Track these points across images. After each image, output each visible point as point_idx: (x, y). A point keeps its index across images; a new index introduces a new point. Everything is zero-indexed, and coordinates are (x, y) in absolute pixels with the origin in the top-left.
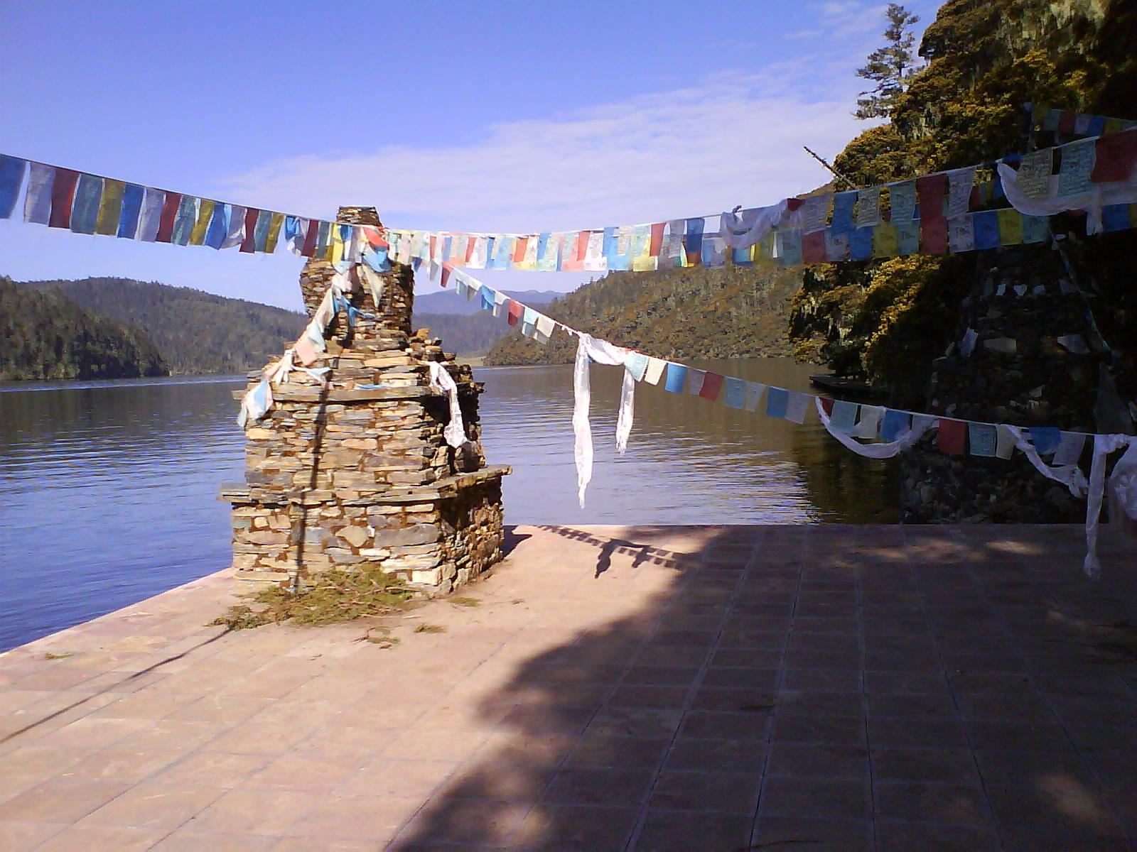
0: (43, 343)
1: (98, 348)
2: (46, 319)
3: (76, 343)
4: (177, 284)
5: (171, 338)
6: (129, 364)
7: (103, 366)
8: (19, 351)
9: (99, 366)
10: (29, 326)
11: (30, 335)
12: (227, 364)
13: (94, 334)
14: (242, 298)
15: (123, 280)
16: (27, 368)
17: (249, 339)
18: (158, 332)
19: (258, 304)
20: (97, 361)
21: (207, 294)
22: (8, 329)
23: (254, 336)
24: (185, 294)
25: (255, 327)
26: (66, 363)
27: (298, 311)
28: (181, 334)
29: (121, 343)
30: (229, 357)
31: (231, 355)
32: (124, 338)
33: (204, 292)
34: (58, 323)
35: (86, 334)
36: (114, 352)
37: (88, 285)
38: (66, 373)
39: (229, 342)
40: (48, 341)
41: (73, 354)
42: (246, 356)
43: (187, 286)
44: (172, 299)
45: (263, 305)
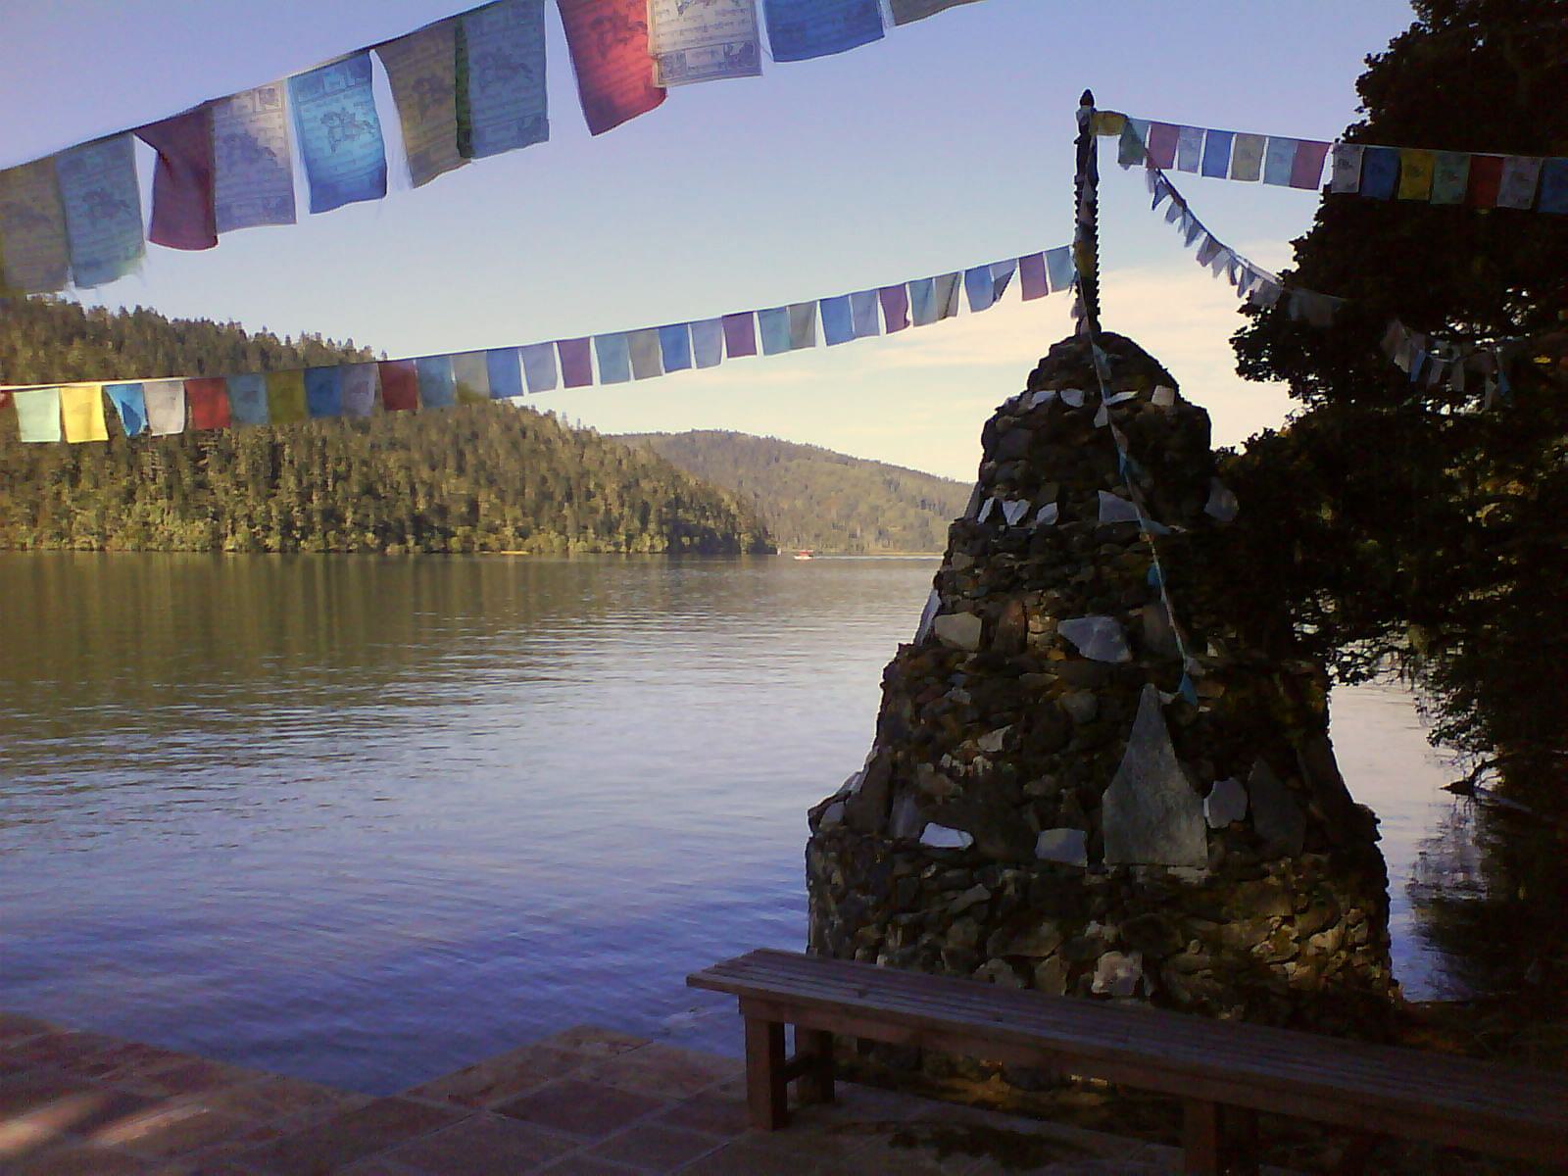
0: (626, 509)
1: (690, 516)
2: (631, 480)
3: (664, 510)
4: (798, 440)
5: (786, 507)
6: (727, 538)
7: (697, 540)
8: (600, 517)
9: (691, 540)
10: (612, 488)
11: (613, 500)
12: (854, 542)
13: (686, 499)
14: (878, 459)
15: (732, 433)
16: (607, 538)
17: (884, 511)
18: (770, 498)
19: (898, 467)
20: (689, 534)
21: (834, 452)
22: (588, 490)
23: (891, 508)
24: (808, 452)
25: (894, 496)
26: (652, 533)
27: (949, 477)
28: (799, 503)
29: (719, 511)
30: (858, 532)
31: (861, 530)
32: (723, 505)
33: (829, 450)
34: (645, 485)
35: (678, 499)
36: (711, 523)
37: (690, 441)
38: (652, 546)
39: (859, 515)
40: (632, 506)
41: (661, 522)
42: (880, 533)
43: (809, 443)
44: (790, 459)
45: (904, 468)
